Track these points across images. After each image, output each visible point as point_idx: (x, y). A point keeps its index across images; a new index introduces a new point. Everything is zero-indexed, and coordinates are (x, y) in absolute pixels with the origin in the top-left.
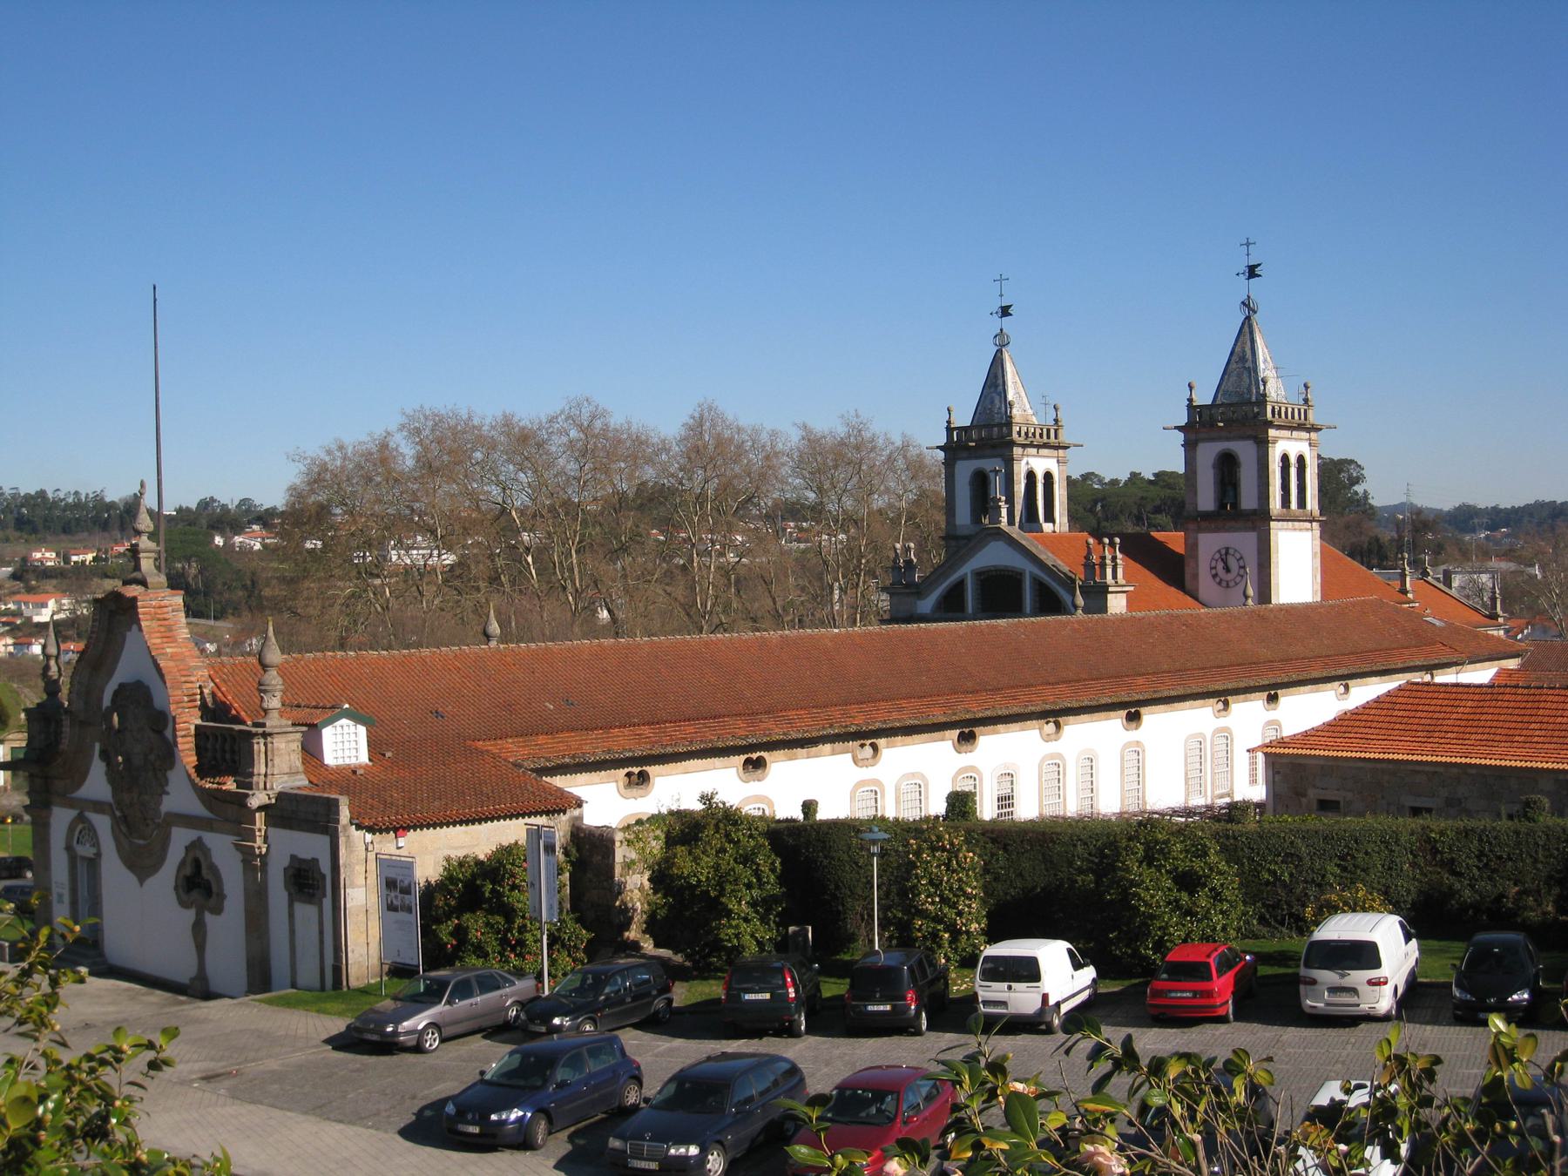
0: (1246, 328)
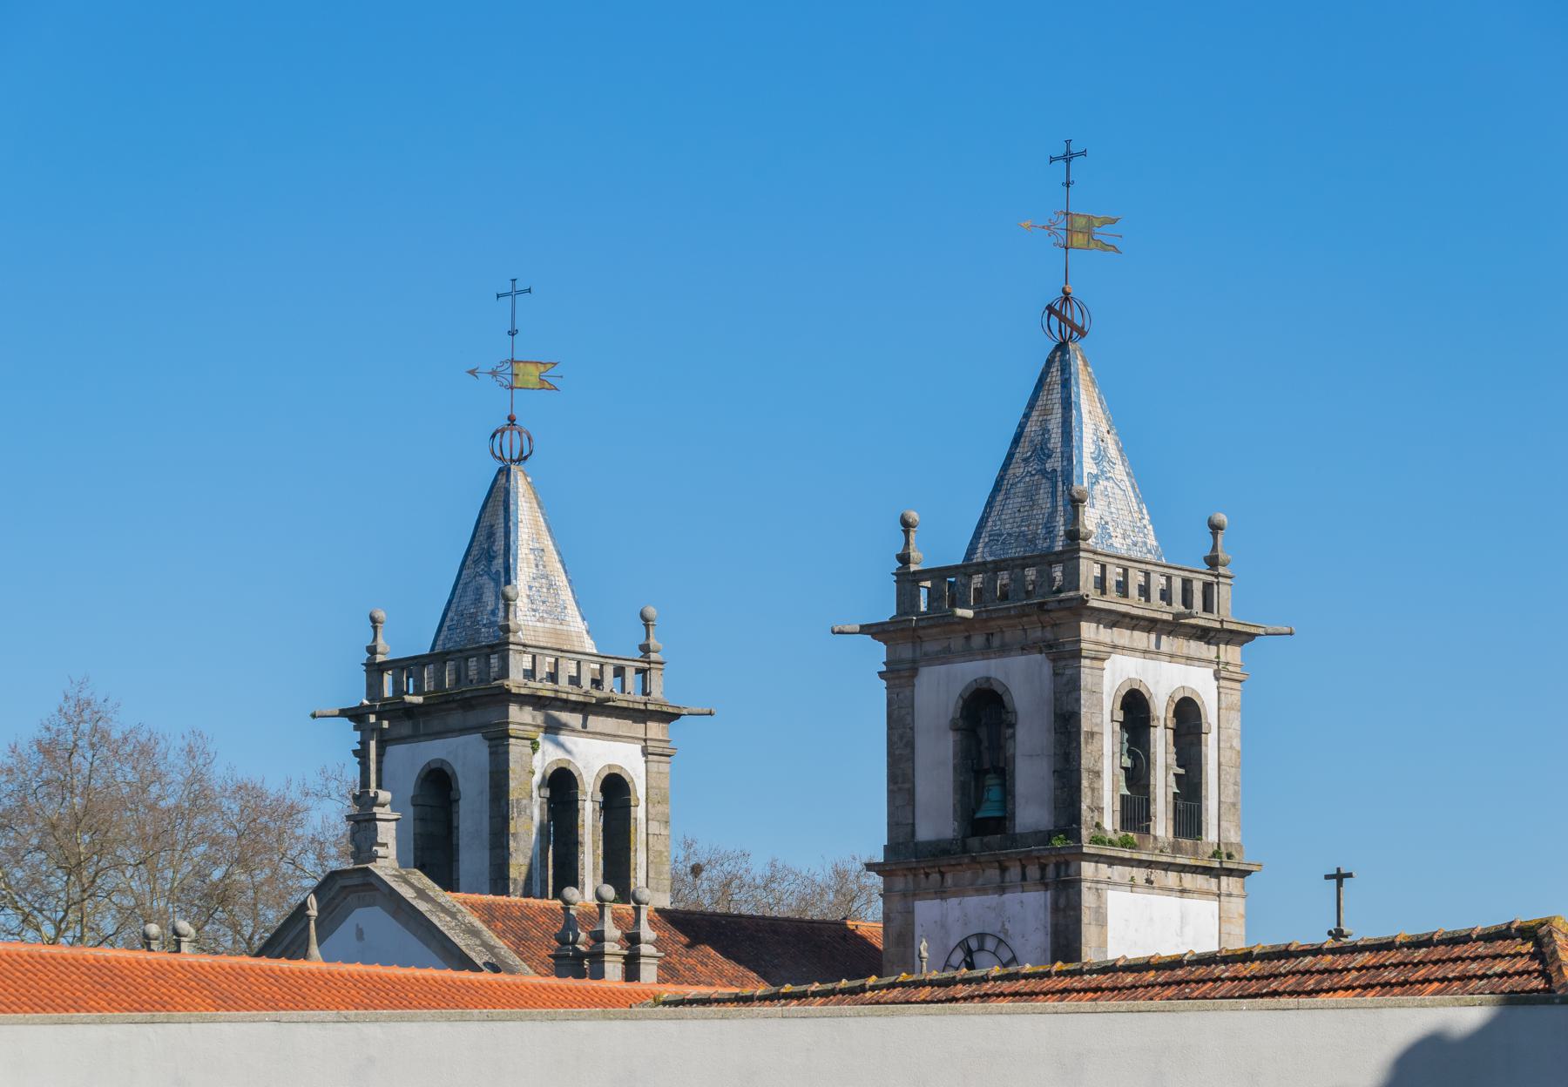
0: (1055, 375)
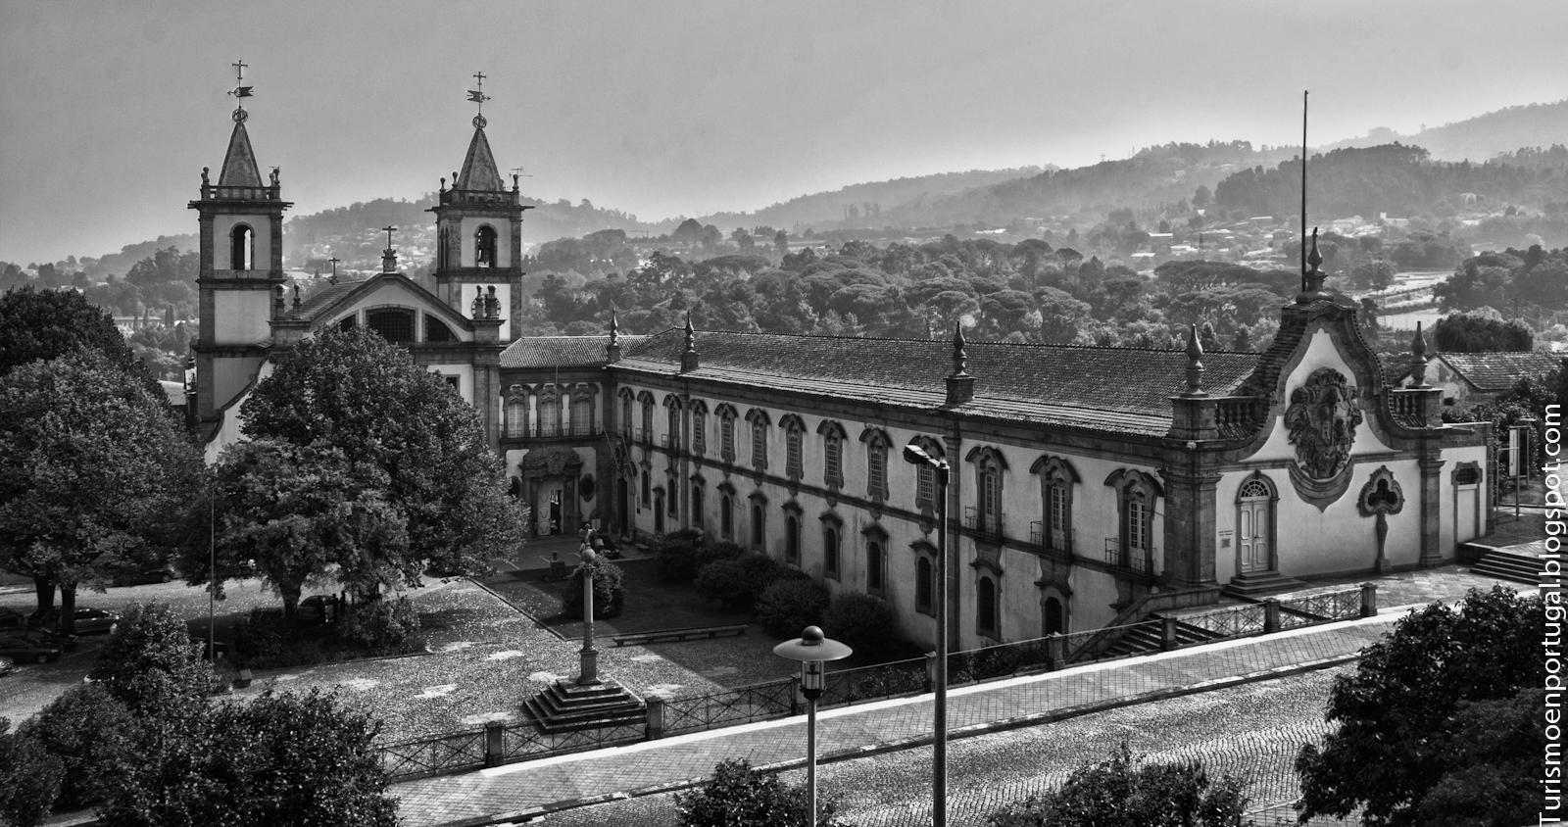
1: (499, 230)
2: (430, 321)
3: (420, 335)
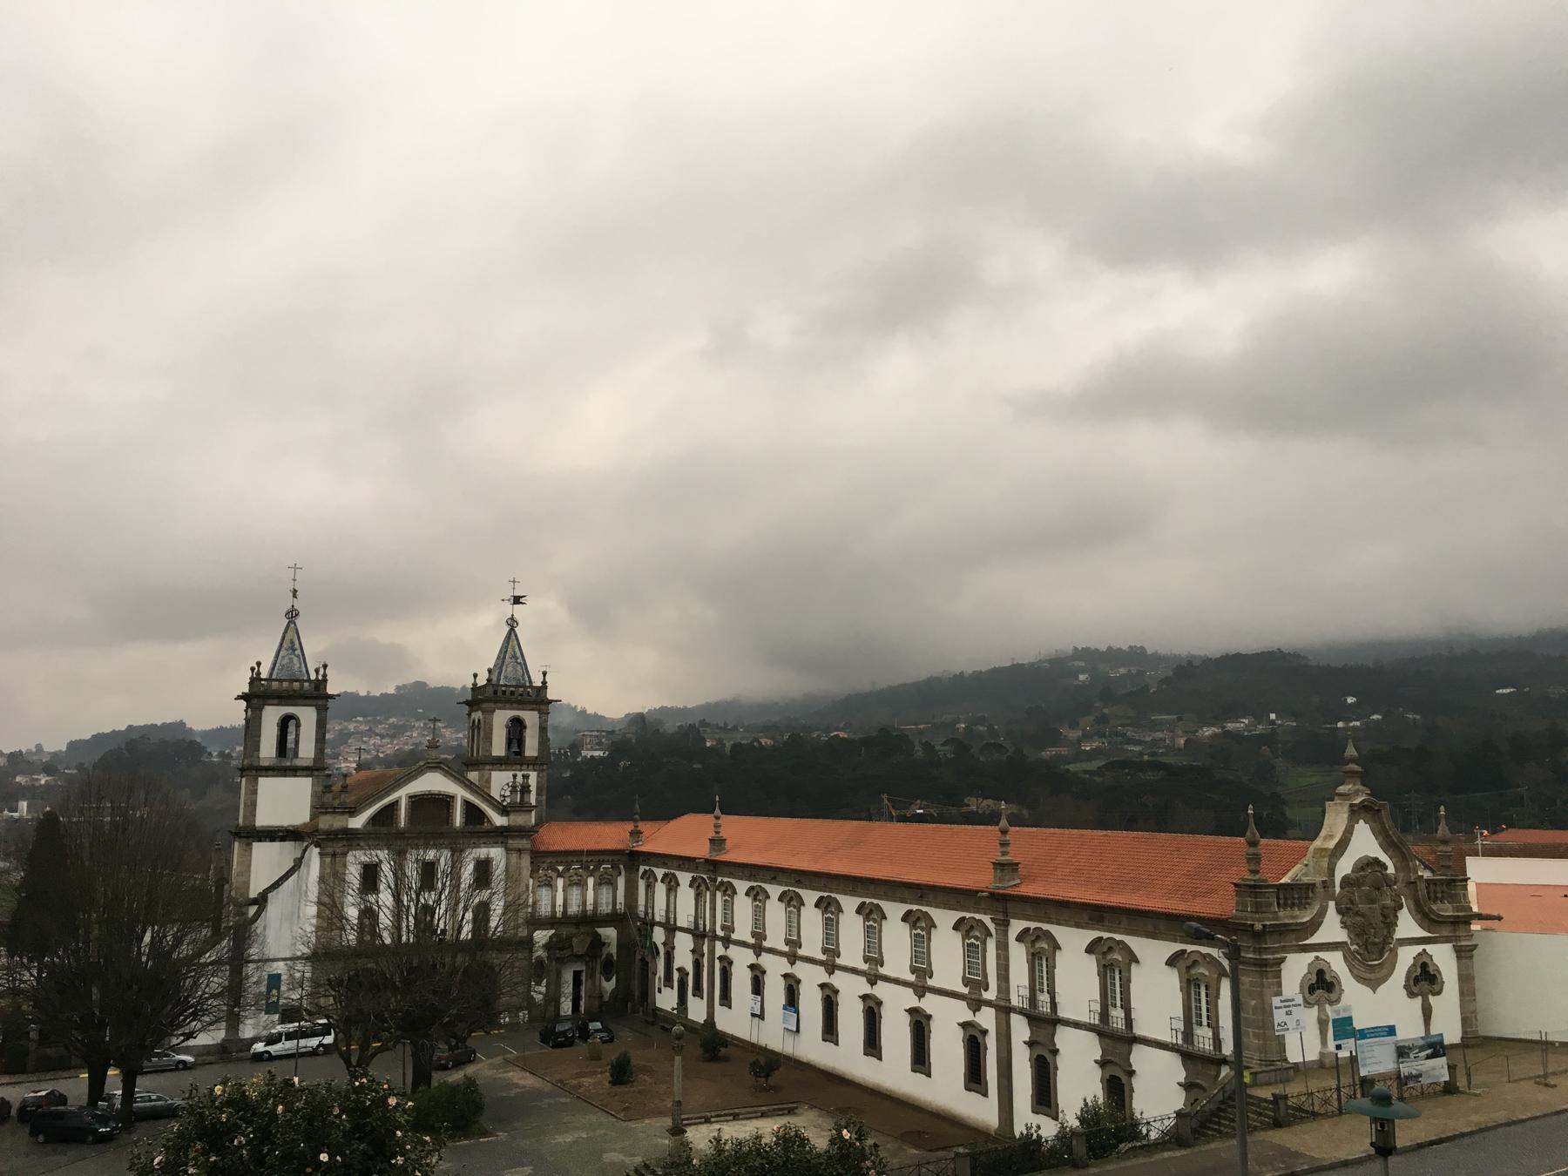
0: (513, 634)
1: (528, 723)
2: (469, 807)
3: (458, 819)
